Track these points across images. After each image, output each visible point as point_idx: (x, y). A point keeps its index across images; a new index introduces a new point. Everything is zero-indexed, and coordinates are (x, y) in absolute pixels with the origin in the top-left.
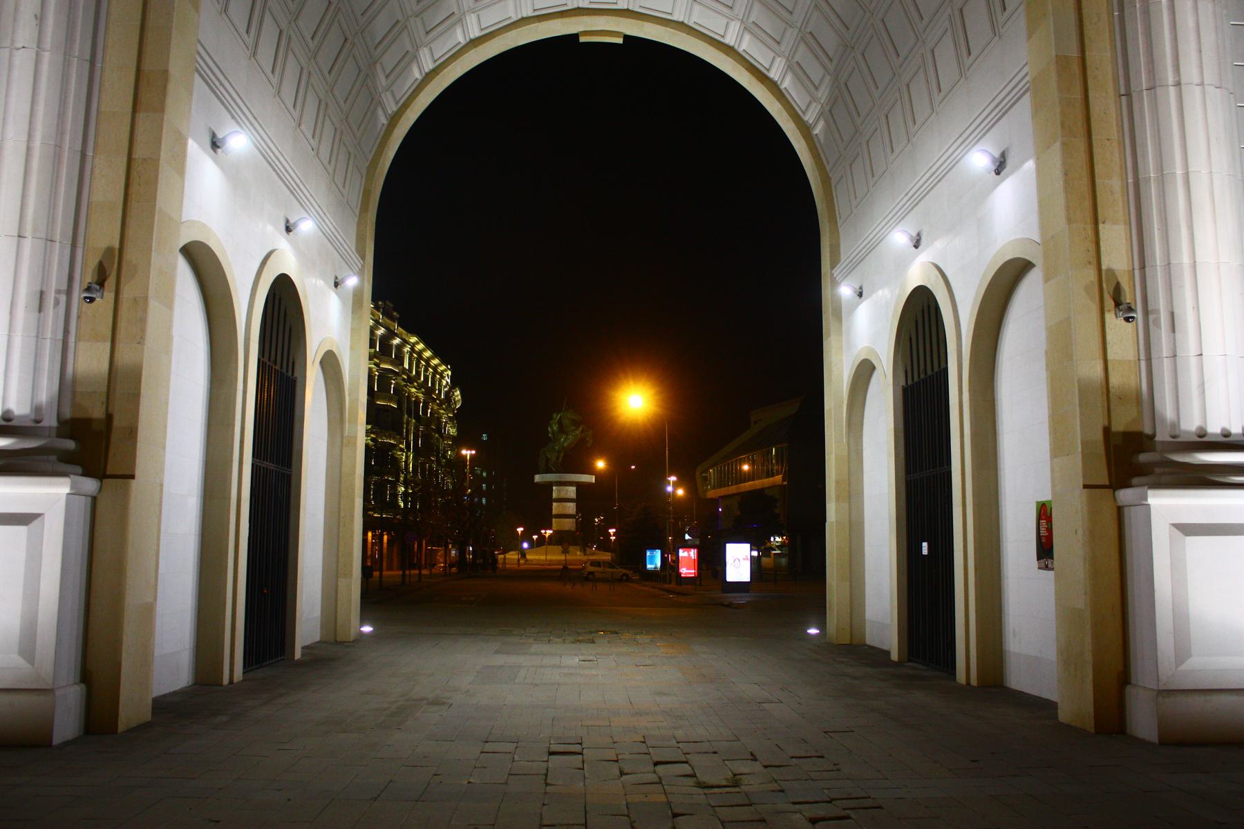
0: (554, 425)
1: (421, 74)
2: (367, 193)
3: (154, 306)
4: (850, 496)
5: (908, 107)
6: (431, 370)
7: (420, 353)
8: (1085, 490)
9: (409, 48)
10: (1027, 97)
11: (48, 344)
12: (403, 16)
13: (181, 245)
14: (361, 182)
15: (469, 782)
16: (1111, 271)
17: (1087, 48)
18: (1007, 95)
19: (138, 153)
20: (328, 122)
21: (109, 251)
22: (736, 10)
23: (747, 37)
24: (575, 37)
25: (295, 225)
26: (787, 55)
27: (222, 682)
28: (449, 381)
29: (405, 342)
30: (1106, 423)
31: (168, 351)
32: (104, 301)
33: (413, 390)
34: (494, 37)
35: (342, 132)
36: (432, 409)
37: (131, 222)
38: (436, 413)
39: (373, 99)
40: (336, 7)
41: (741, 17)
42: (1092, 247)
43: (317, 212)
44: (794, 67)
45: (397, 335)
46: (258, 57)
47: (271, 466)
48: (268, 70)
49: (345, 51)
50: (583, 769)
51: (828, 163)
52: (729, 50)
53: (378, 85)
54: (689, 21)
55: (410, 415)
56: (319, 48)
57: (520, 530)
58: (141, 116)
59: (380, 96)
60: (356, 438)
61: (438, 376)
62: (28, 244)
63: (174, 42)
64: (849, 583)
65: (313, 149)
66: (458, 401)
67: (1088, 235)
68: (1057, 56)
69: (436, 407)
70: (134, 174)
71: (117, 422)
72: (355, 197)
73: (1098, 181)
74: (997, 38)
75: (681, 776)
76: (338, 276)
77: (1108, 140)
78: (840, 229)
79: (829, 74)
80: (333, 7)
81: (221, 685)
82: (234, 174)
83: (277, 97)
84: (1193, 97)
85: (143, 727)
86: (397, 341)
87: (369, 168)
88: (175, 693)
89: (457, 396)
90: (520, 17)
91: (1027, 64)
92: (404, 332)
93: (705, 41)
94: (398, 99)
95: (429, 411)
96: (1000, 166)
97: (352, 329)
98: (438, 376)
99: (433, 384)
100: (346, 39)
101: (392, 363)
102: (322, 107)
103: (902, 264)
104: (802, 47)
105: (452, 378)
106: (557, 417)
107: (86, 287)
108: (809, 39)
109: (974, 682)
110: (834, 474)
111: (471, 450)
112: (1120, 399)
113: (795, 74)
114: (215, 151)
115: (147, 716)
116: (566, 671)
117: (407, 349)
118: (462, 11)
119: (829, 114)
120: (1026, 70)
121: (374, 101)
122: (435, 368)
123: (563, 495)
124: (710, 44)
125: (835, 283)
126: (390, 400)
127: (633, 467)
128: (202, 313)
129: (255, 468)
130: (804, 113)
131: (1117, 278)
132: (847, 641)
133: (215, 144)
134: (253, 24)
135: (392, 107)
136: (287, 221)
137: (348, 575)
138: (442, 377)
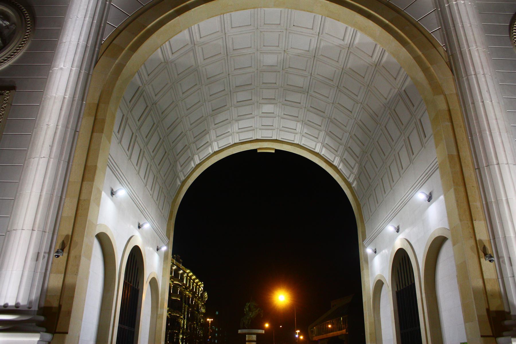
0: (247, 308)
2: (171, 213)
3: (83, 260)
4: (376, 340)
5: (390, 176)
6: (195, 284)
7: (191, 277)
10: (438, 171)
11: (38, 275)
12: (188, 143)
13: (96, 234)
14: (169, 208)
16: (481, 241)
17: (460, 151)
19: (83, 197)
21: (67, 236)
22: (319, 138)
23: (324, 149)
24: (256, 150)
25: (142, 225)
26: (340, 156)
28: (202, 289)
29: (184, 272)
30: (487, 307)
31: (87, 278)
32: (63, 257)
33: (188, 293)
35: (163, 188)
36: (195, 301)
37: (77, 226)
38: (197, 303)
39: (175, 175)
40: (162, 140)
42: (471, 231)
43: (151, 220)
44: (344, 161)
45: (181, 269)
46: (132, 159)
47: (126, 327)
48: (135, 165)
49: (165, 156)
51: (359, 198)
52: (317, 154)
54: (301, 143)
55: (185, 304)
56: (155, 155)
58: (85, 183)
59: (178, 174)
60: (163, 315)
61: (198, 287)
62: (35, 233)
65: (151, 195)
66: (206, 297)
69: (197, 300)
70: (80, 206)
71: (63, 309)
72: (167, 214)
73: (471, 203)
74: (423, 148)
78: (365, 225)
82: (119, 206)
83: (138, 175)
84: (505, 169)
86: (181, 272)
89: (206, 295)
90: (234, 143)
91: (436, 158)
92: (184, 268)
95: (194, 302)
96: (430, 198)
97: (163, 268)
98: (198, 287)
101: (179, 281)
102: (155, 179)
103: (392, 239)
104: (346, 153)
105: (204, 287)
106: (248, 304)
107: (56, 251)
108: (349, 149)
110: (368, 330)
111: (211, 319)
112: (492, 296)
113: (343, 163)
114: (112, 196)
117: (185, 275)
118: (211, 141)
119: (358, 178)
120: (437, 160)
121: (176, 176)
122: (197, 283)
123: (251, 339)
124: (310, 152)
125: (365, 247)
126: (177, 297)
127: (281, 326)
128: (102, 262)
130: (348, 178)
131: (483, 243)
133: (112, 193)
134: (131, 146)
135: (184, 178)
136: (139, 224)
138: (200, 287)
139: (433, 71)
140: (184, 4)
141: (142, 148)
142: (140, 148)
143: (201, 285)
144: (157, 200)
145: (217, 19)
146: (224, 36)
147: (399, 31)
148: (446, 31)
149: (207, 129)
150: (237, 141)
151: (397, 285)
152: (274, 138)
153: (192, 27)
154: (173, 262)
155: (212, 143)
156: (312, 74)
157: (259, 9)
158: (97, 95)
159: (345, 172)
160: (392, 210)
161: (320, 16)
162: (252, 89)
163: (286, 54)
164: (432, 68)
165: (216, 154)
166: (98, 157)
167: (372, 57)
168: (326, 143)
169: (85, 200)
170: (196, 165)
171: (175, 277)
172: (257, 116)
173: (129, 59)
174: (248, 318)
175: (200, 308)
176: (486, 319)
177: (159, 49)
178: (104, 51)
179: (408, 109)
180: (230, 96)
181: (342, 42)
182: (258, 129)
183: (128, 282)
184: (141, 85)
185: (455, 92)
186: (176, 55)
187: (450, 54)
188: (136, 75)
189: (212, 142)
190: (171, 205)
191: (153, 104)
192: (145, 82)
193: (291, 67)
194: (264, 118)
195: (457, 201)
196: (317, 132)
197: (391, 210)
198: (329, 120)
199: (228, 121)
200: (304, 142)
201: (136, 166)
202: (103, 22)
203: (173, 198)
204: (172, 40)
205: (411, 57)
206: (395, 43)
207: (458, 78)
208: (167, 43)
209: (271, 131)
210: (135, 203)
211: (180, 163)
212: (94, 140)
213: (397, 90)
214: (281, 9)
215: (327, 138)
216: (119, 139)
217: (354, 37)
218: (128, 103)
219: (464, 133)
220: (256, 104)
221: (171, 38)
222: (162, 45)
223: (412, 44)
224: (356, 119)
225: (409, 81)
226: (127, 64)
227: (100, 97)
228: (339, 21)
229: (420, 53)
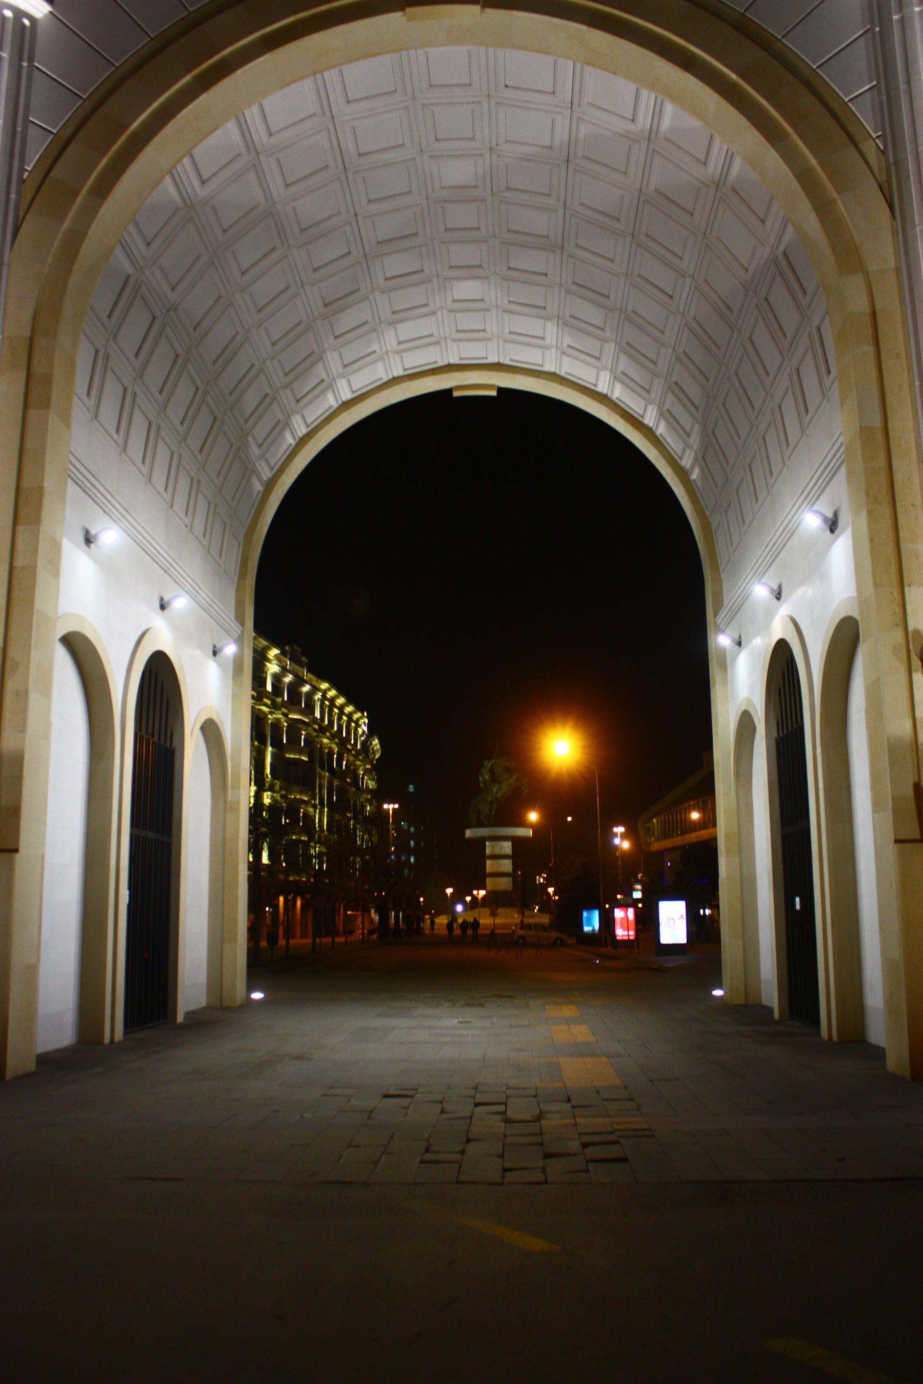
1: (295, 440)
3: (33, 697)
4: (740, 851)
7: (332, 701)
12: (272, 389)
17: (889, 420)
18: (833, 457)
19: (19, 562)
22: (604, 358)
24: (449, 391)
25: (169, 603)
27: (103, 1039)
28: (365, 729)
29: (315, 689)
30: (916, 779)
31: (46, 735)
33: (325, 741)
35: (216, 505)
36: (347, 761)
37: (13, 625)
38: (352, 765)
41: (609, 366)
42: (898, 610)
44: (665, 414)
45: (306, 682)
47: (151, 835)
48: (139, 462)
49: (215, 429)
51: (707, 507)
52: (603, 399)
53: (251, 454)
54: (560, 370)
56: (189, 430)
57: (449, 891)
58: (20, 529)
59: (254, 464)
61: (353, 725)
63: (48, 458)
64: (741, 942)
65: (186, 526)
66: (377, 750)
67: (895, 599)
68: (861, 427)
69: (351, 759)
70: (15, 581)
72: (232, 563)
73: (903, 546)
78: (722, 576)
79: (698, 422)
80: (200, 393)
82: (107, 567)
85: (27, 1076)
86: (306, 688)
87: (246, 535)
89: (376, 745)
90: (390, 377)
91: (841, 433)
94: (272, 465)
95: (344, 763)
96: (833, 525)
97: (234, 695)
99: (348, 733)
100: (215, 419)
101: (302, 712)
102: (194, 487)
103: (769, 615)
104: (670, 395)
105: (369, 726)
108: (675, 388)
109: (835, 1038)
110: (723, 829)
111: (394, 803)
115: (32, 1066)
116: (438, 1031)
117: (319, 696)
118: (331, 377)
119: (702, 460)
120: (841, 439)
121: (248, 470)
122: (350, 716)
123: (497, 851)
126: (301, 752)
127: (569, 819)
129: (133, 838)
130: (681, 458)
132: (743, 1002)
133: (89, 540)
134: (123, 424)
135: (267, 474)
137: (234, 940)
138: (358, 725)
139: (843, 210)
140: (217, 58)
142: (148, 419)
143: (362, 721)
145: (307, 85)
146: (331, 125)
147: (765, 103)
148: (888, 93)
149: (316, 350)
150: (398, 372)
151: (778, 724)
152: (492, 359)
153: (246, 113)
154: (284, 664)
155: (333, 383)
156: (568, 205)
157: (412, 52)
158: (28, 314)
159: (673, 442)
160: (767, 547)
161: (571, 64)
162: (420, 246)
163: (495, 157)
164: (840, 203)
165: (348, 409)
166: (42, 467)
167: (705, 164)
168: (622, 372)
170: (297, 439)
171: (291, 704)
173: (94, 217)
174: (489, 799)
175: (363, 778)
177: (168, 180)
178: (33, 199)
179: (794, 298)
180: (365, 266)
181: (630, 127)
182: (448, 341)
184: (129, 269)
185: (892, 264)
186: (212, 186)
187: (891, 160)
188: (118, 251)
189: (334, 379)
190: (242, 543)
191: (168, 311)
192: (140, 260)
193: (512, 189)
195: (872, 540)
196: (598, 344)
198: (622, 316)
199: (366, 327)
200: (567, 367)
201: (141, 466)
202: (20, 121)
203: (247, 524)
204: (198, 152)
206: (752, 136)
207: (904, 229)
208: (186, 161)
209: (481, 345)
211: (255, 439)
213: (767, 250)
214: (468, 48)
215: (623, 359)
216: (91, 409)
217: (658, 113)
218: (106, 321)
219: (906, 371)
220: (435, 281)
221: (194, 146)
222: (175, 166)
224: (685, 315)
225: (790, 233)
226: (90, 232)
227: (35, 319)
228: (615, 73)
229: (814, 162)
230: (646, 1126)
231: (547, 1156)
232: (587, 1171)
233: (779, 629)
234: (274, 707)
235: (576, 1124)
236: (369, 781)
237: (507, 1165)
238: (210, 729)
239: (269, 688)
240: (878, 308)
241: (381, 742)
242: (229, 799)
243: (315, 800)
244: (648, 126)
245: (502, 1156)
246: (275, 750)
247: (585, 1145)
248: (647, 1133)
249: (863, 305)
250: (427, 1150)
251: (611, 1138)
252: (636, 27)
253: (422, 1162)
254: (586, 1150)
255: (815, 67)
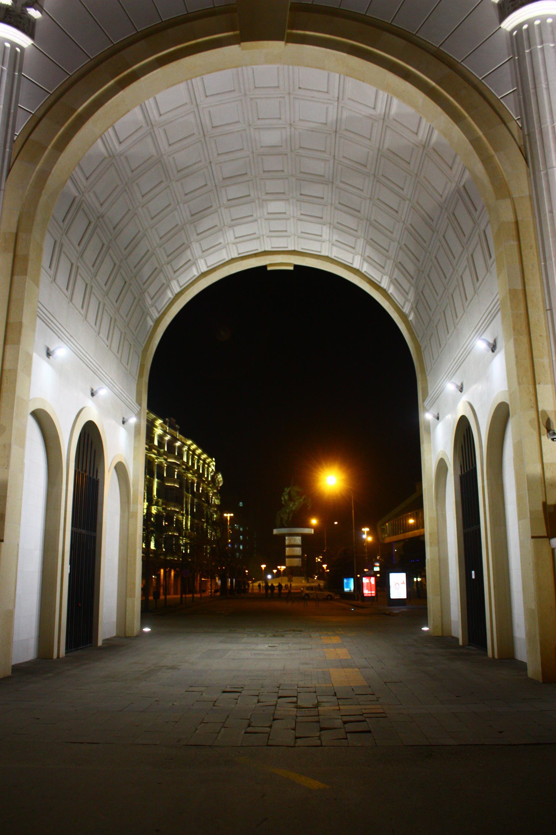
1: (173, 295)
2: (142, 367)
3: (15, 449)
7: (194, 451)
8: (533, 539)
9: (164, 281)
15: (173, 704)
16: (544, 412)
17: (526, 285)
18: (493, 308)
20: (116, 329)
24: (265, 267)
25: (96, 392)
27: (53, 657)
28: (214, 468)
29: (184, 444)
30: (544, 500)
33: (190, 475)
34: (215, 271)
35: (125, 333)
36: (203, 487)
39: (144, 312)
41: (360, 253)
42: (533, 398)
43: (110, 382)
44: (394, 282)
45: (178, 440)
46: (74, 301)
47: (84, 532)
48: (79, 307)
50: (237, 699)
52: (356, 272)
53: (147, 303)
57: (263, 566)
58: (8, 347)
59: (148, 310)
60: (137, 513)
61: (206, 466)
63: (25, 306)
64: (439, 598)
65: (107, 346)
66: (221, 481)
68: (510, 289)
69: (205, 486)
72: (135, 370)
73: (535, 360)
75: (289, 703)
76: (125, 417)
77: (540, 336)
80: (116, 267)
81: (53, 659)
82: (60, 371)
83: (86, 322)
86: (178, 444)
87: (143, 351)
88: (26, 663)
89: (220, 478)
90: (230, 258)
93: (341, 266)
94: (159, 310)
95: (201, 489)
96: (493, 348)
99: (203, 471)
101: (176, 458)
103: (456, 401)
104: (396, 270)
105: (216, 466)
108: (399, 266)
109: (496, 657)
111: (230, 513)
112: (552, 485)
114: (49, 358)
115: (10, 673)
117: (185, 448)
118: (195, 257)
119: (416, 308)
120: (498, 296)
121: (145, 314)
122: (204, 460)
123: (293, 542)
125: (426, 410)
126: (174, 482)
127: (336, 523)
130: (403, 307)
131: (547, 415)
134: (70, 284)
135: (156, 315)
136: (92, 390)
137: (133, 596)
138: (209, 466)
139: (498, 161)
140: (129, 70)
141: (88, 282)
142: (85, 282)
143: (211, 463)
144: (118, 352)
145: (183, 86)
146: (196, 110)
148: (524, 94)
149: (186, 242)
150: (235, 255)
152: (291, 248)
153: (146, 102)
154: (165, 429)
156: (336, 157)
157: (244, 68)
158: (15, 219)
159: (398, 298)
160: (454, 360)
161: (337, 75)
162: (248, 181)
163: (293, 129)
164: (496, 157)
165: (204, 277)
166: (22, 310)
168: (368, 256)
169: (10, 370)
170: (174, 295)
172: (261, 218)
173: (55, 163)
174: (288, 511)
175: (212, 498)
176: (542, 516)
177: (99, 141)
179: (470, 213)
180: (215, 192)
181: (372, 112)
182: (265, 237)
183: (82, 470)
184: (77, 194)
185: (528, 193)
186: (124, 146)
187: (526, 133)
188: (69, 183)
189: (196, 259)
190: (140, 356)
191: (98, 218)
194: (273, 221)
196: (353, 239)
197: (453, 360)
198: (368, 223)
199: (216, 228)
200: (335, 253)
201: (81, 310)
203: (144, 345)
204: (117, 125)
205: (467, 140)
206: (444, 118)
207: (534, 173)
209: (285, 239)
210: (84, 362)
212: (15, 286)
213: (454, 185)
214: (277, 66)
215: (369, 249)
216: (52, 276)
217: (389, 104)
218: (61, 223)
219: (536, 257)
220: (257, 201)
221: (115, 122)
222: (103, 133)
223: (470, 119)
224: (406, 222)
225: (467, 174)
226: (53, 172)
228: (364, 81)
229: (480, 133)
230: (382, 711)
231: (322, 729)
232: (347, 739)
233: (461, 410)
234: (159, 454)
235: (339, 710)
236: (215, 500)
237: (297, 735)
238: (120, 468)
239: (156, 443)
240: (519, 219)
241: (223, 477)
242: (131, 510)
243: (183, 511)
244: (383, 111)
245: (294, 729)
246: (159, 481)
247: (345, 723)
248: (383, 715)
249: (511, 218)
250: (249, 726)
251: (361, 718)
252: (377, 55)
253: (246, 733)
254: (346, 725)
255: (480, 79)
